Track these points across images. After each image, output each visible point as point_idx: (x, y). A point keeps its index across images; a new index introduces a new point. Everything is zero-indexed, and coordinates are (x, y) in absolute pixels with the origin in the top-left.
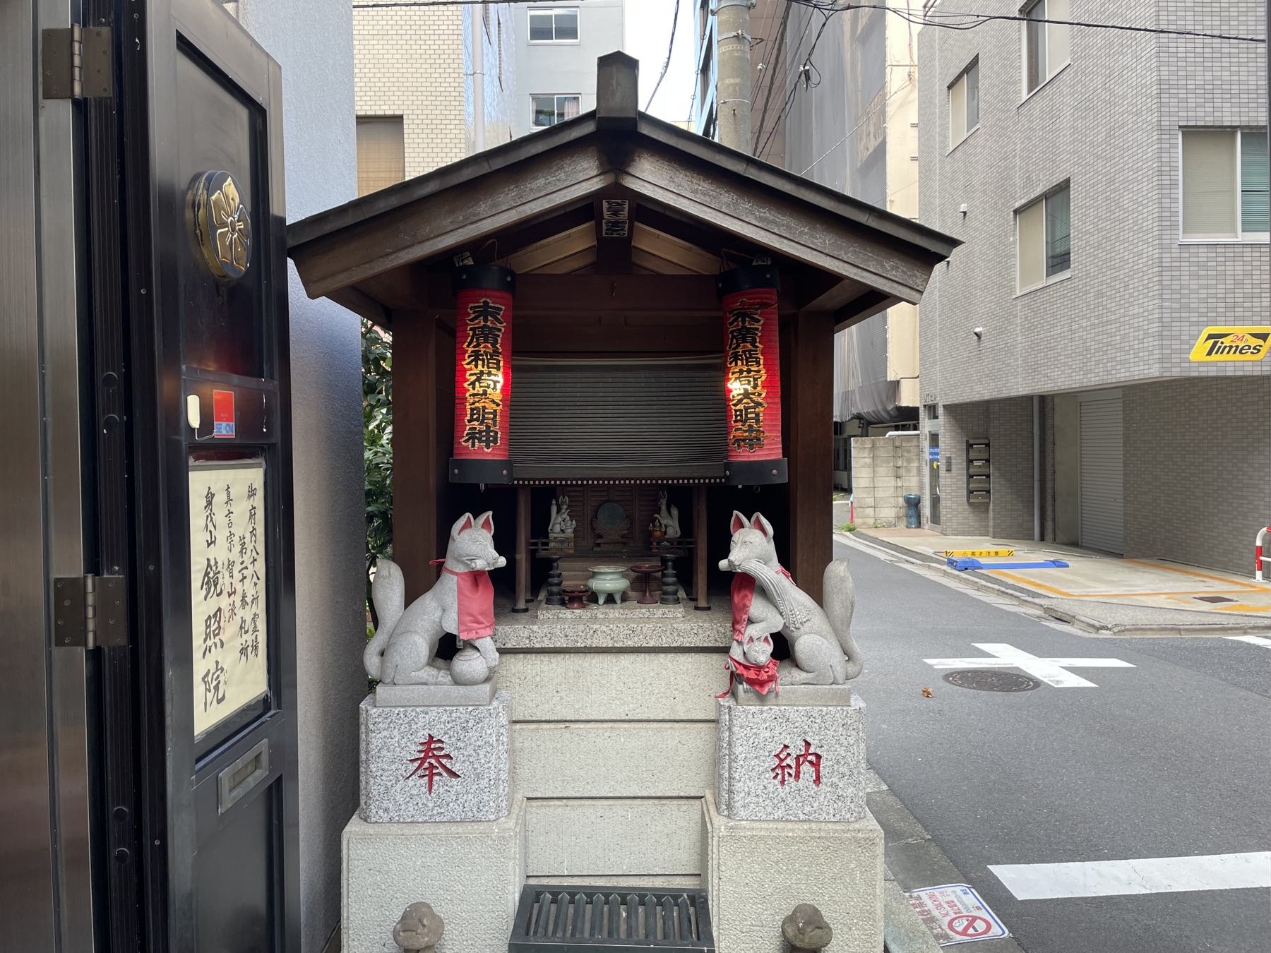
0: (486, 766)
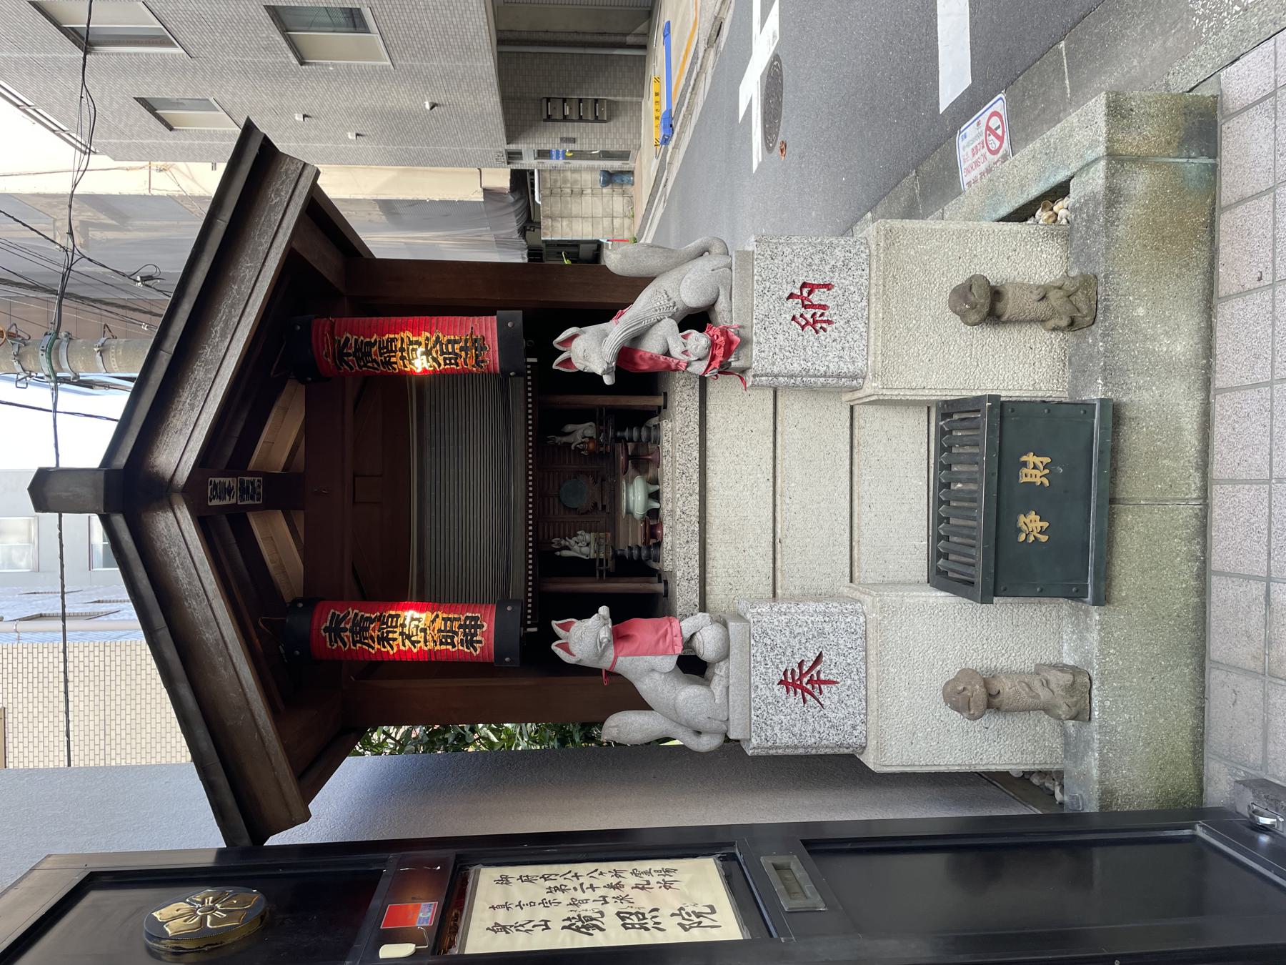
0: (811, 625)
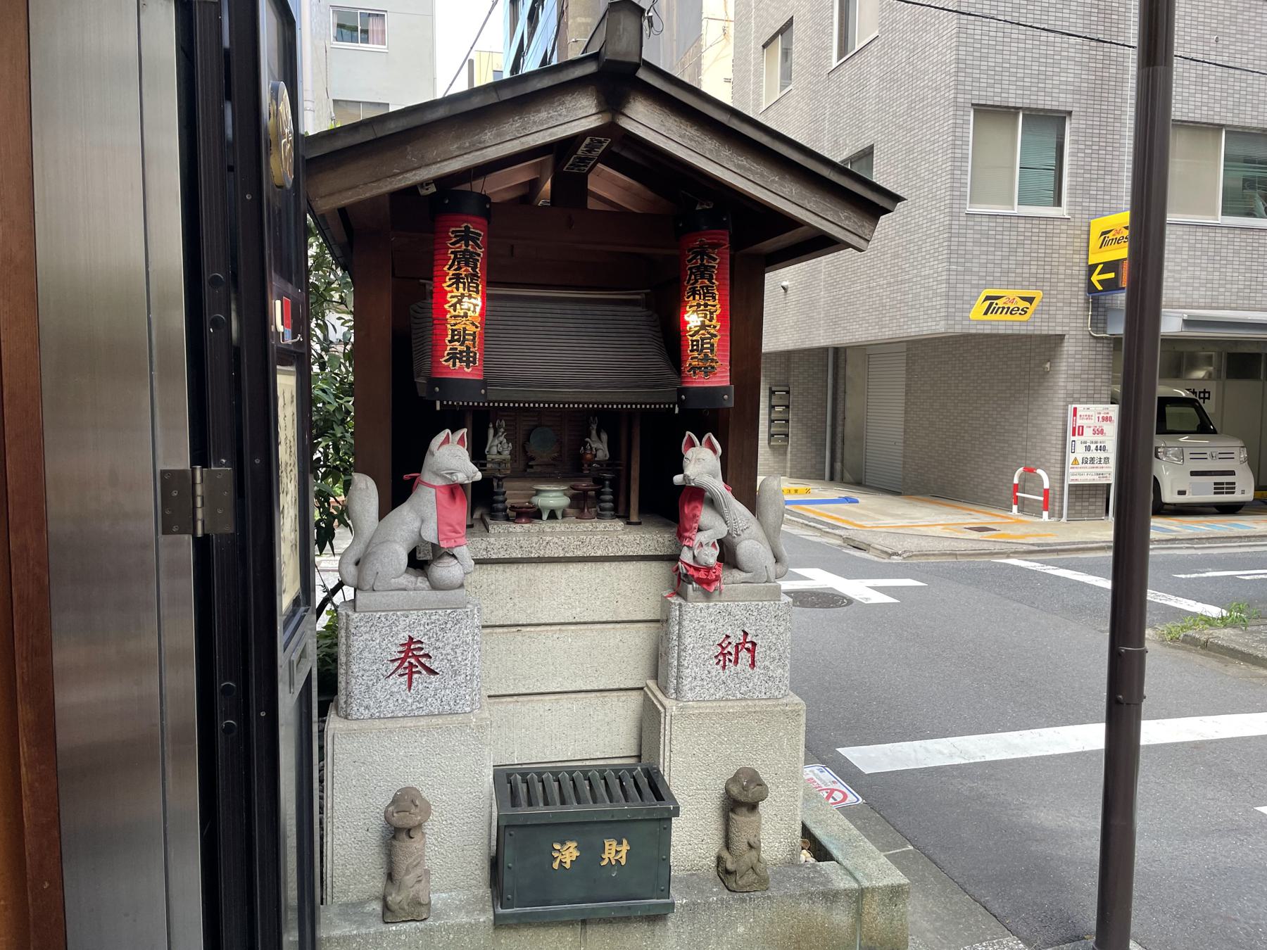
0: (463, 663)
